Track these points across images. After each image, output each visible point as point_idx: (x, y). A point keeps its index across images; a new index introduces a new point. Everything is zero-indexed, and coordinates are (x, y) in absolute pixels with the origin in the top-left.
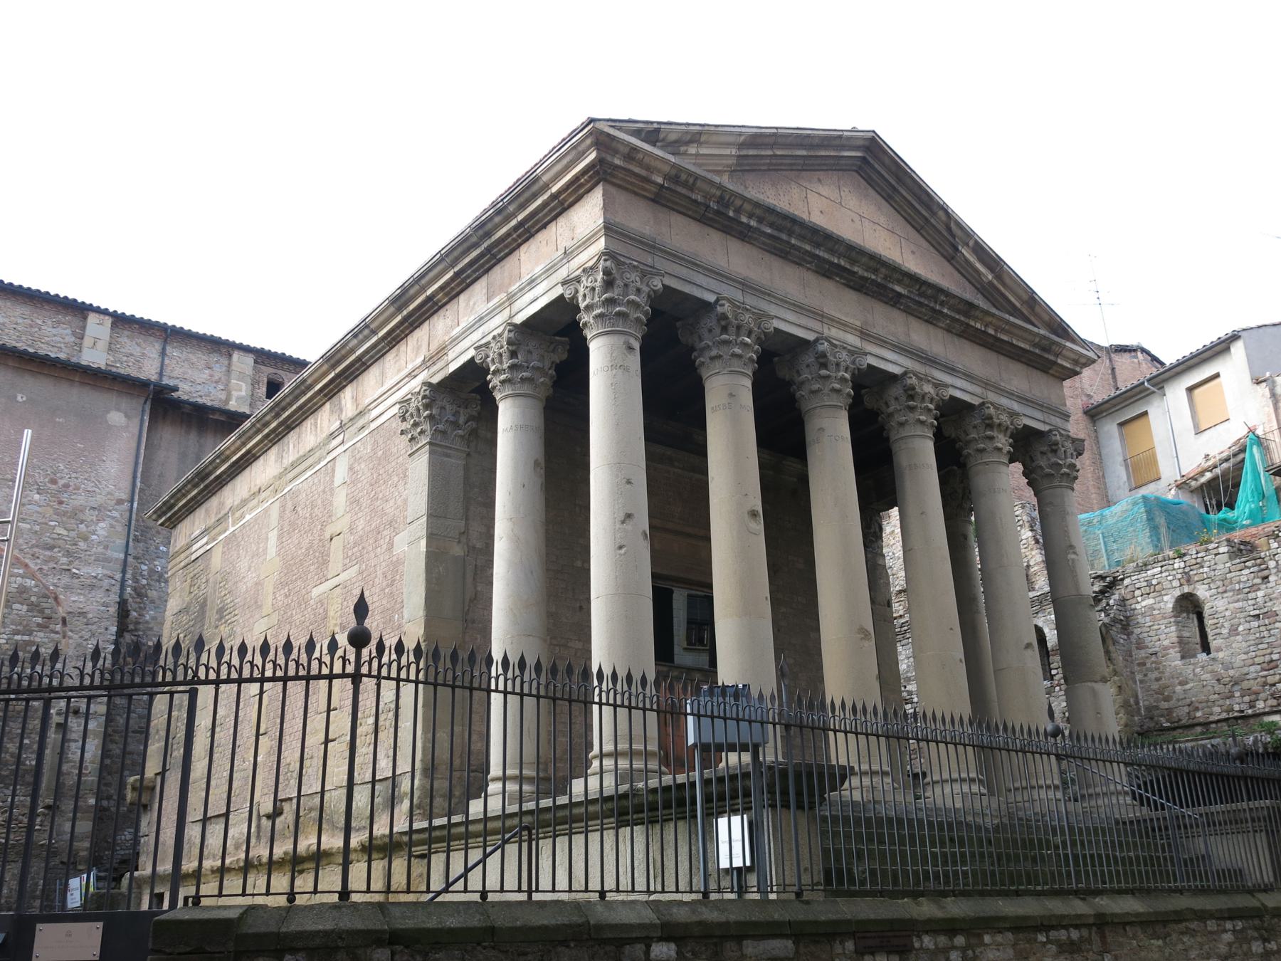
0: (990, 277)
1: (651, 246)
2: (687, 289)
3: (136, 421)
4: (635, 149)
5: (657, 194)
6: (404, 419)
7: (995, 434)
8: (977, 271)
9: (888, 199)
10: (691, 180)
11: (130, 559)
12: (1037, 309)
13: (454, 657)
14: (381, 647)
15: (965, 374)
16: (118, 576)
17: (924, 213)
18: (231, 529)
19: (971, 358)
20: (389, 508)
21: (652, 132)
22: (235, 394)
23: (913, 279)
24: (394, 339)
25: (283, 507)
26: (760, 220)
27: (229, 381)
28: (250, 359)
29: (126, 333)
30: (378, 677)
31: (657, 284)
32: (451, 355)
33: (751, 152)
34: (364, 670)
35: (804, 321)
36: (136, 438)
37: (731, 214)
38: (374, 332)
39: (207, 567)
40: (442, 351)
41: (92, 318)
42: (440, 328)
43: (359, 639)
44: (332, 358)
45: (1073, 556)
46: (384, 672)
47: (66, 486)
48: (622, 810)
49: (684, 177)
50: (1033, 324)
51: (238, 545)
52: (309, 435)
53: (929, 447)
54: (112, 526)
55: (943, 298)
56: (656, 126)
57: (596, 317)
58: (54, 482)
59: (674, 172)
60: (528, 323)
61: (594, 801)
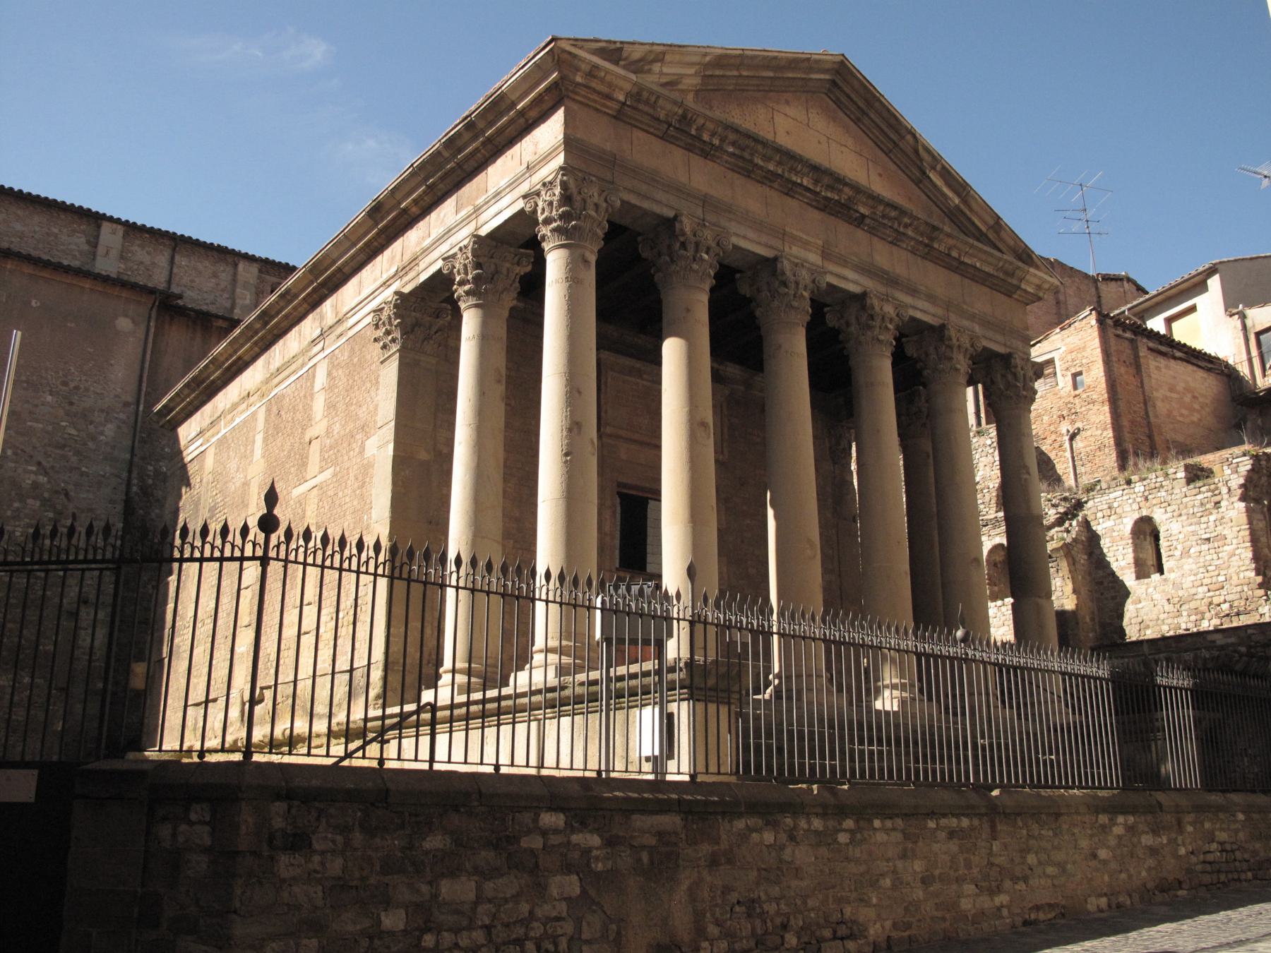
0: (957, 201)
1: (612, 161)
2: (646, 205)
3: (143, 327)
4: (596, 67)
5: (619, 111)
6: (377, 327)
8: (944, 195)
9: (857, 121)
10: (653, 99)
11: (136, 459)
12: (1003, 234)
13: (325, 539)
14: (289, 534)
15: (925, 294)
16: (125, 475)
17: (892, 136)
18: (223, 432)
19: (935, 278)
20: (362, 413)
21: (613, 52)
22: (239, 302)
23: (876, 199)
24: (372, 251)
25: (269, 411)
27: (233, 291)
28: (254, 269)
29: (138, 242)
30: (286, 561)
32: (422, 265)
33: (717, 72)
34: (272, 554)
36: (142, 343)
37: (693, 132)
38: (354, 245)
39: (202, 468)
40: (414, 260)
41: (106, 227)
42: (413, 239)
43: (268, 523)
44: (316, 268)
45: (1026, 476)
46: (292, 557)
47: (77, 388)
48: (556, 701)
49: (645, 94)
50: (1000, 250)
51: (228, 448)
52: (292, 343)
53: (887, 365)
54: (119, 427)
55: (906, 220)
56: (618, 45)
57: (553, 230)
58: (65, 384)
59: (635, 90)
60: (493, 235)
61: (539, 692)
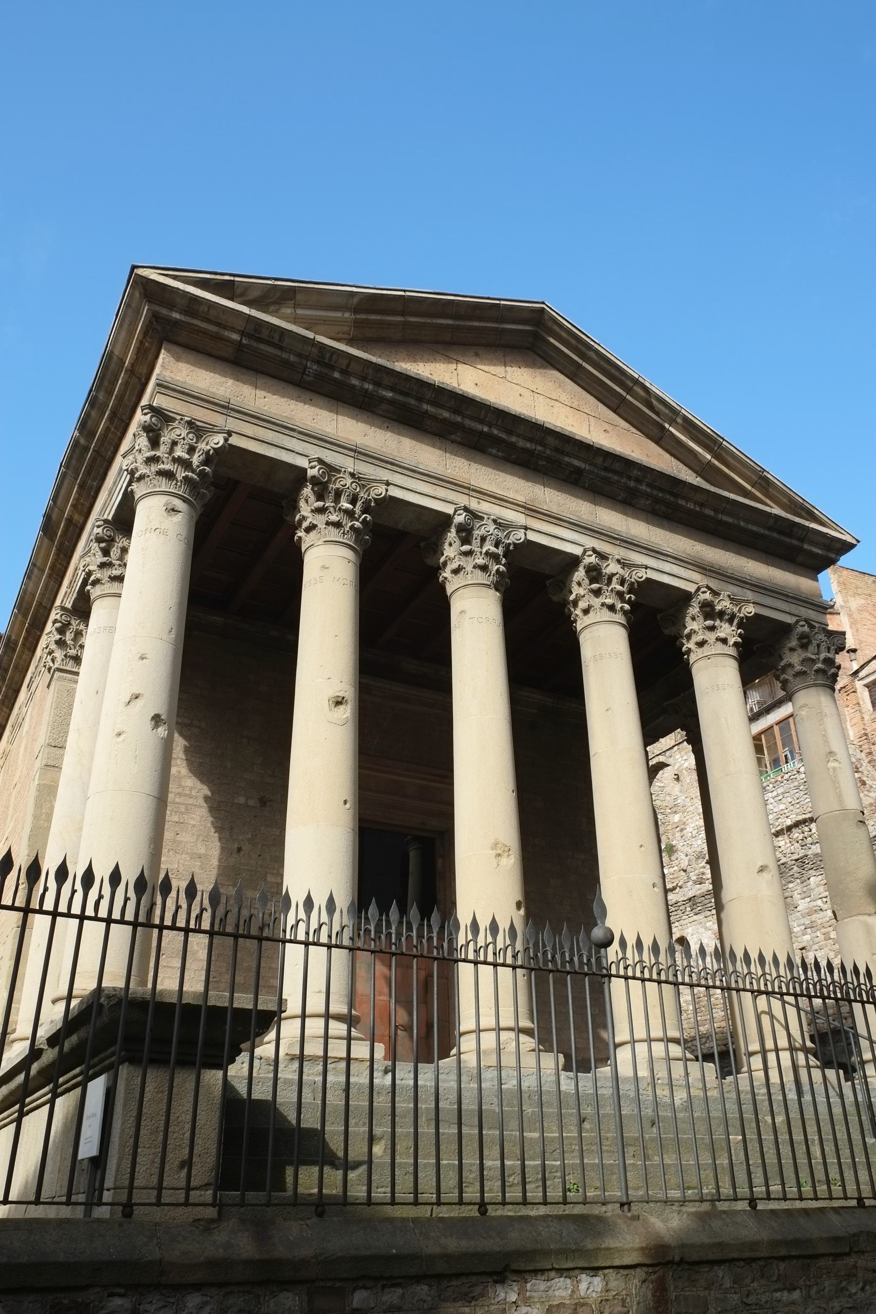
0: (709, 457)
7: (717, 623)
21: (226, 288)
26: (378, 384)
31: (218, 440)
33: (373, 317)
35: (441, 493)
